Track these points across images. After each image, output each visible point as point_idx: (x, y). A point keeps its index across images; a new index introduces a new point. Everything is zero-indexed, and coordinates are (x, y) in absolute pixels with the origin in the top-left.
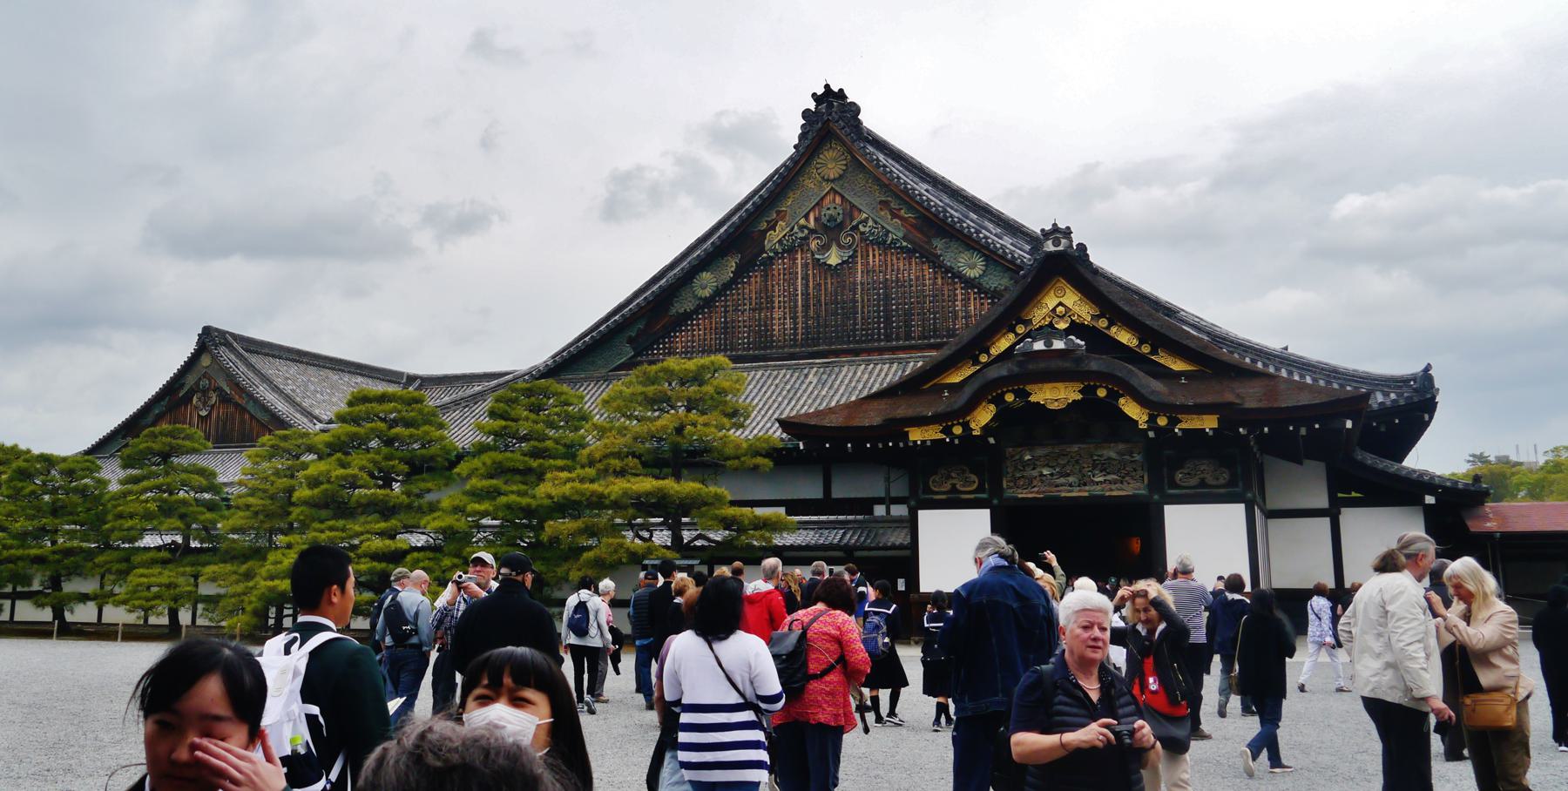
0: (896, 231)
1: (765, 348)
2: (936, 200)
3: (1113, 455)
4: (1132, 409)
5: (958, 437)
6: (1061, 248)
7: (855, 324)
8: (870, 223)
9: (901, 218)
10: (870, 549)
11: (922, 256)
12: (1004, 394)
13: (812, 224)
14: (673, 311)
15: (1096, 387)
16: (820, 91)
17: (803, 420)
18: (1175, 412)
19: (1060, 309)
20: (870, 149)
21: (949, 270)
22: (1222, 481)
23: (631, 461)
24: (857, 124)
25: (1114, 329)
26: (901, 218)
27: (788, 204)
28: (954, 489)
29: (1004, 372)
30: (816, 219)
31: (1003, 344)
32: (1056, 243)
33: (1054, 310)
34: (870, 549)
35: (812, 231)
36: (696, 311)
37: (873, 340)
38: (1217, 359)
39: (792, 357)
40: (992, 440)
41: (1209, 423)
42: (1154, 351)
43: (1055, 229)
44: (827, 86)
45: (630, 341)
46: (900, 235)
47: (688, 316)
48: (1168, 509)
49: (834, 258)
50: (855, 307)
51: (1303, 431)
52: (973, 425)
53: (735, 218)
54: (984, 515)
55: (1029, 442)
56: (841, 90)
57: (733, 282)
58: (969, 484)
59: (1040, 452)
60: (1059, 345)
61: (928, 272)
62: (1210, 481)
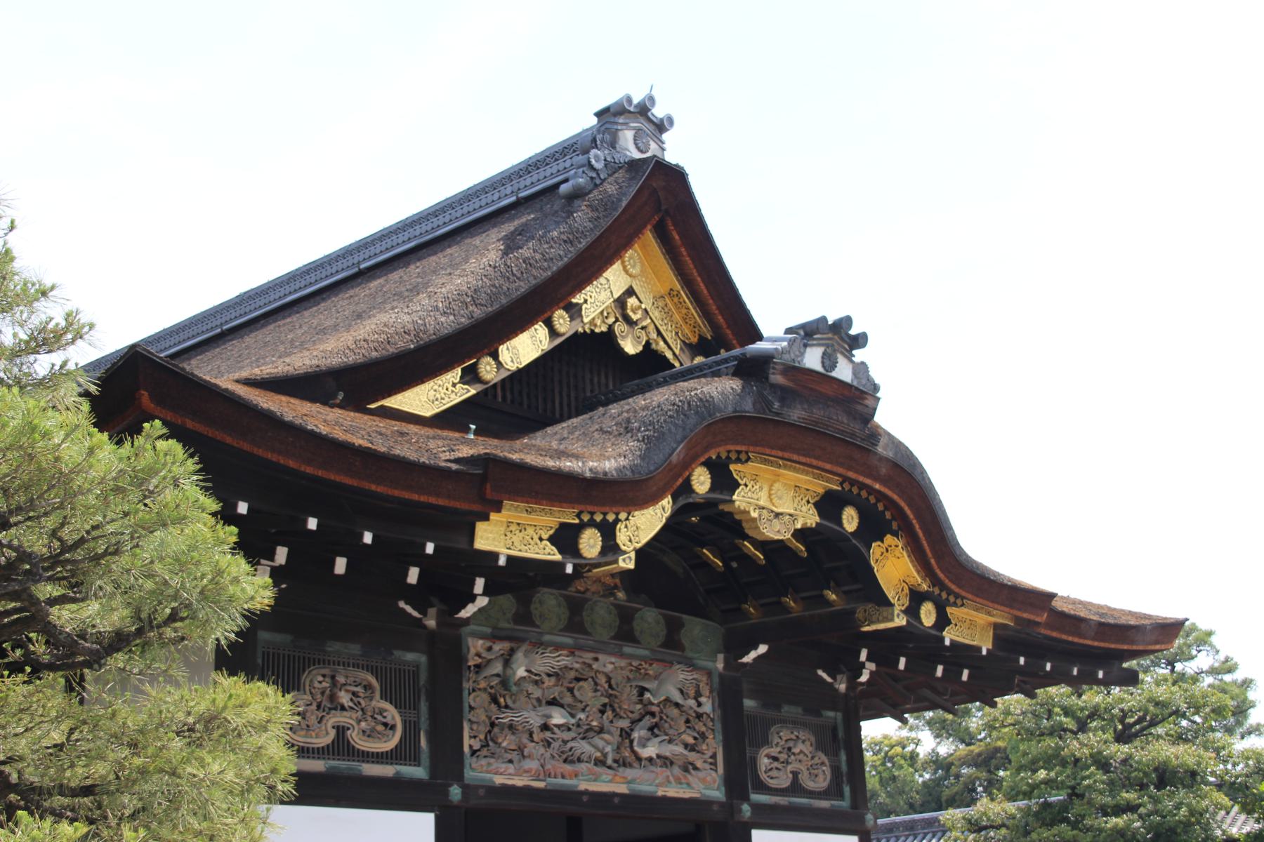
43: (643, 110)
52: (622, 537)
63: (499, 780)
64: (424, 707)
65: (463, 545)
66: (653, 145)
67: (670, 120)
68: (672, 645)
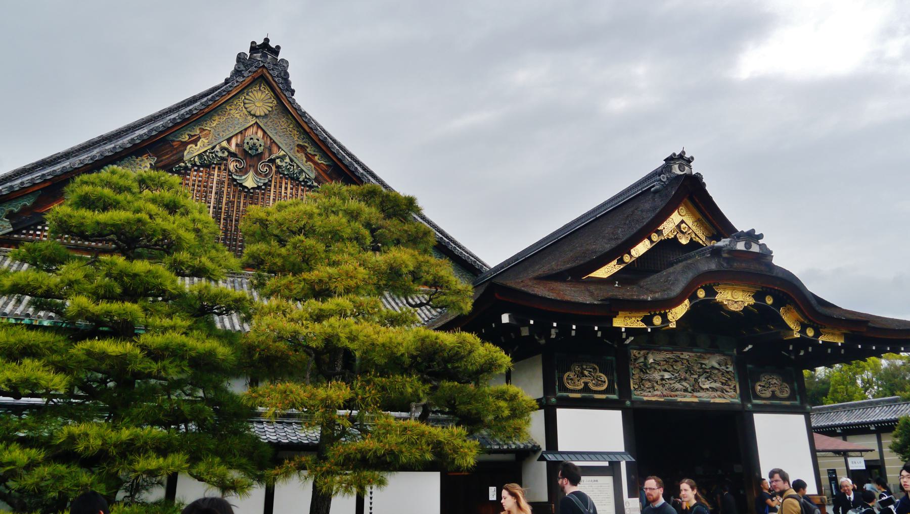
5: (656, 330)
16: (260, 42)
22: (786, 395)
27: (214, 123)
28: (586, 389)
30: (237, 145)
35: (231, 154)
44: (267, 40)
45: (10, 216)
46: (313, 176)
49: (250, 181)
54: (615, 417)
59: (660, 357)
62: (778, 393)
63: (645, 399)
64: (615, 375)
65: (609, 326)
66: (687, 168)
68: (713, 349)
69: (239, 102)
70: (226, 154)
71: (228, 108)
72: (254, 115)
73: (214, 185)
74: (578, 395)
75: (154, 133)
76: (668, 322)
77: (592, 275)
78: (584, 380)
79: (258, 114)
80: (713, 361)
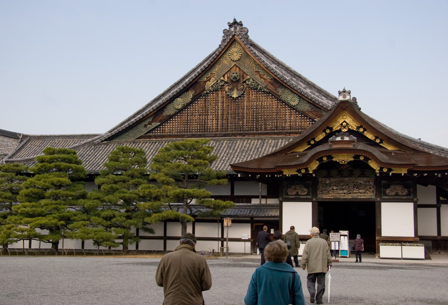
0: (262, 83)
1: (205, 131)
2: (280, 72)
3: (362, 182)
4: (373, 165)
5: (303, 174)
6: (346, 99)
7: (243, 123)
8: (251, 80)
9: (265, 79)
10: (262, 217)
11: (272, 95)
12: (323, 157)
13: (226, 80)
14: (164, 114)
15: (360, 156)
16: (232, 21)
17: (240, 165)
18: (390, 167)
19: (344, 124)
20: (252, 48)
21: (283, 102)
22: (404, 194)
23: (172, 180)
24: (247, 38)
25: (365, 132)
26: (265, 79)
27: (216, 69)
28: (297, 194)
29: (324, 149)
30: (228, 77)
31: (321, 137)
32: (344, 97)
33: (342, 124)
34: (262, 217)
35: (226, 83)
36: (174, 115)
37: (251, 130)
38: (403, 145)
39: (216, 136)
40: (314, 175)
41: (403, 172)
42: (381, 142)
43: (344, 92)
44: (235, 19)
46: (264, 86)
47: (170, 117)
48: (383, 204)
49: (235, 95)
50: (243, 116)
51: (439, 175)
52: (309, 169)
53: (193, 75)
55: (329, 176)
56: (241, 22)
57: (191, 103)
58: (304, 192)
59: (333, 180)
60: (346, 139)
61: (275, 102)
62: (400, 193)
67: (350, 91)
69: (226, 56)
70: (223, 83)
71: (222, 60)
72: (233, 61)
73: (220, 99)
74: (293, 197)
75: (191, 80)
76: (309, 171)
77: (293, 151)
78: (297, 191)
79: (235, 59)
80: (361, 181)
